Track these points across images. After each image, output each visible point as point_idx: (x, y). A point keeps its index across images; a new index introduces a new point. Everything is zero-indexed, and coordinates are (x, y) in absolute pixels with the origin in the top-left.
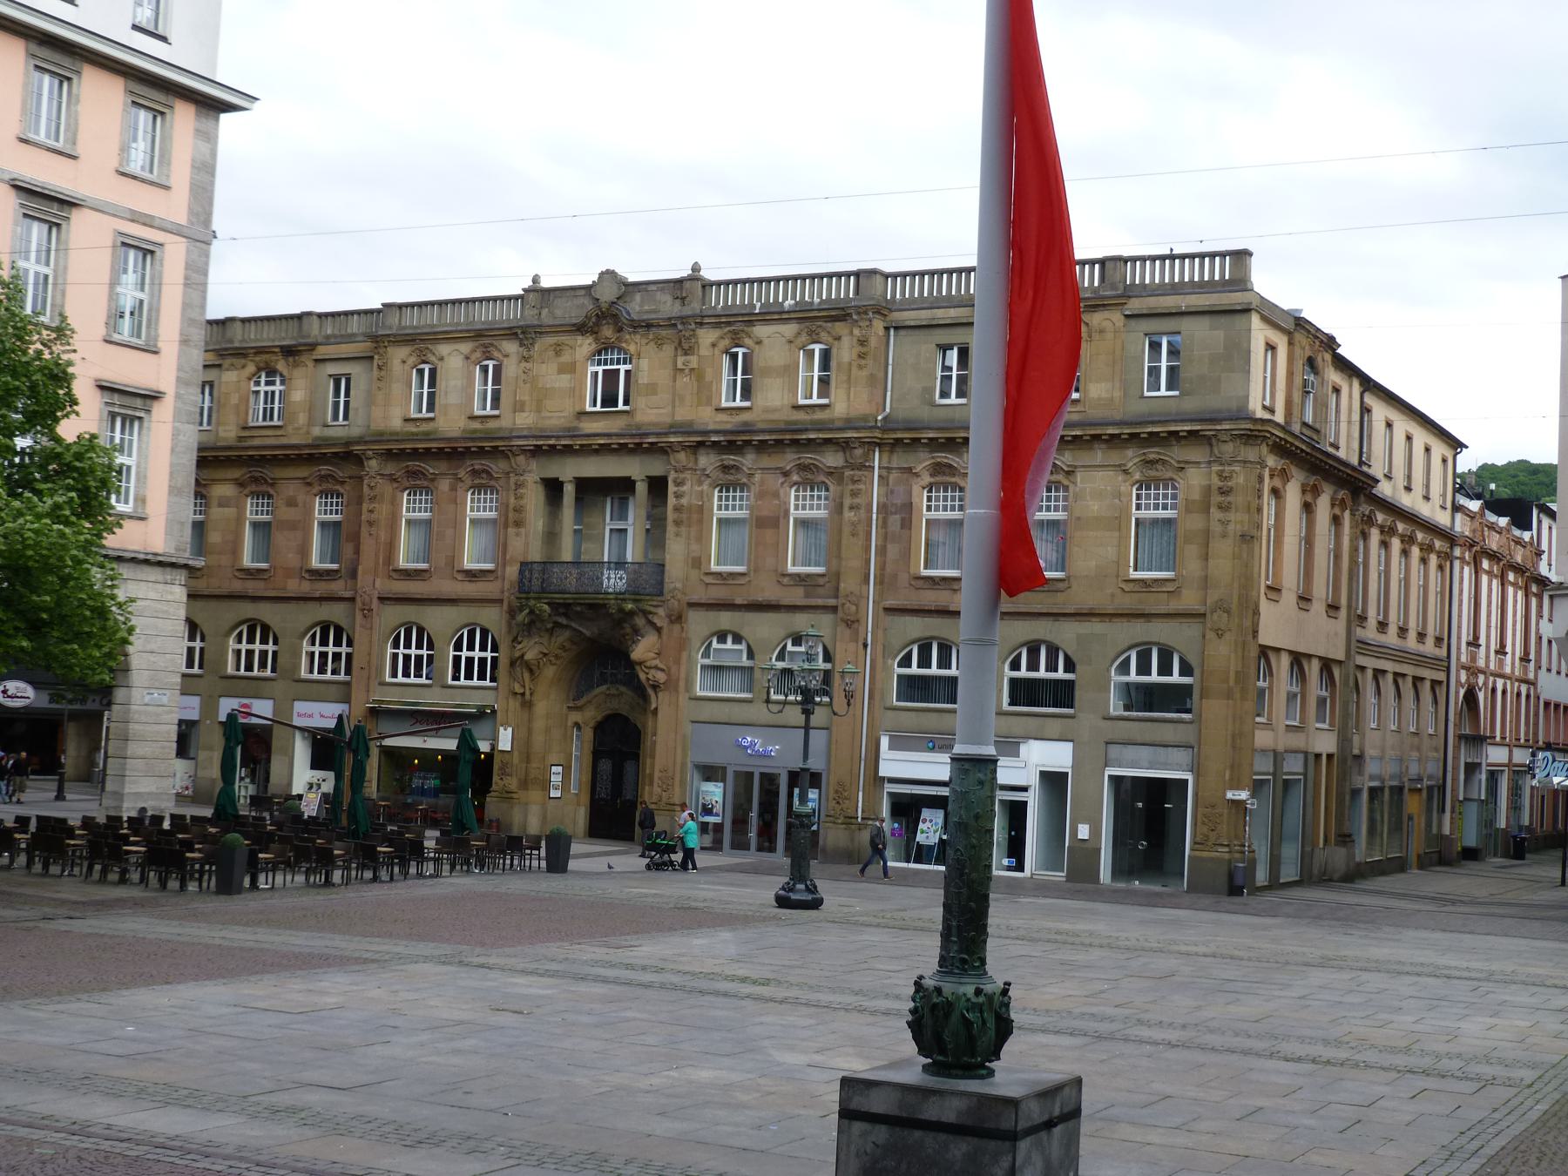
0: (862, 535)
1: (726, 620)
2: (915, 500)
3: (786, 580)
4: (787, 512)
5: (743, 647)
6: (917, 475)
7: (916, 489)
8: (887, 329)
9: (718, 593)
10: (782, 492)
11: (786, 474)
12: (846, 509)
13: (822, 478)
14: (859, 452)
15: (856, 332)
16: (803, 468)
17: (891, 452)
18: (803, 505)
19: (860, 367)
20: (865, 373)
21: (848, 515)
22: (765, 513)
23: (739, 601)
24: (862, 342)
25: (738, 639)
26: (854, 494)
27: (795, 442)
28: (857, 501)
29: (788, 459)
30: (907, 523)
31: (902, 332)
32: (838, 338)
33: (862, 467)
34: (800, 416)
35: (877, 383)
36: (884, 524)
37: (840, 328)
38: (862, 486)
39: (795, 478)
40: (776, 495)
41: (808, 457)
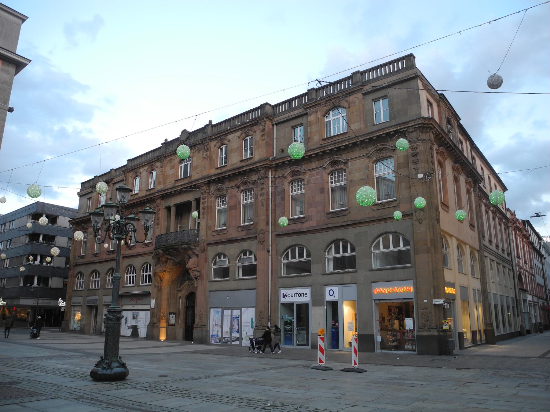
0: (265, 205)
1: (219, 248)
2: (286, 188)
3: (239, 229)
4: (240, 202)
5: (227, 259)
6: (285, 178)
7: (286, 184)
8: (273, 125)
9: (217, 238)
10: (237, 194)
11: (238, 187)
12: (259, 196)
13: (251, 186)
14: (262, 172)
15: (261, 127)
16: (245, 183)
17: (276, 171)
18: (246, 199)
19: (262, 140)
20: (264, 142)
21: (260, 198)
22: (232, 204)
23: (223, 240)
24: (263, 130)
25: (225, 256)
26: (262, 189)
27: (240, 173)
28: (263, 192)
29: (239, 181)
30: (283, 199)
31: (279, 126)
32: (255, 132)
33: (264, 178)
34: (243, 164)
35: (269, 145)
36: (274, 200)
37: (255, 128)
38: (264, 186)
39: (242, 188)
40: (235, 196)
41: (245, 179)
